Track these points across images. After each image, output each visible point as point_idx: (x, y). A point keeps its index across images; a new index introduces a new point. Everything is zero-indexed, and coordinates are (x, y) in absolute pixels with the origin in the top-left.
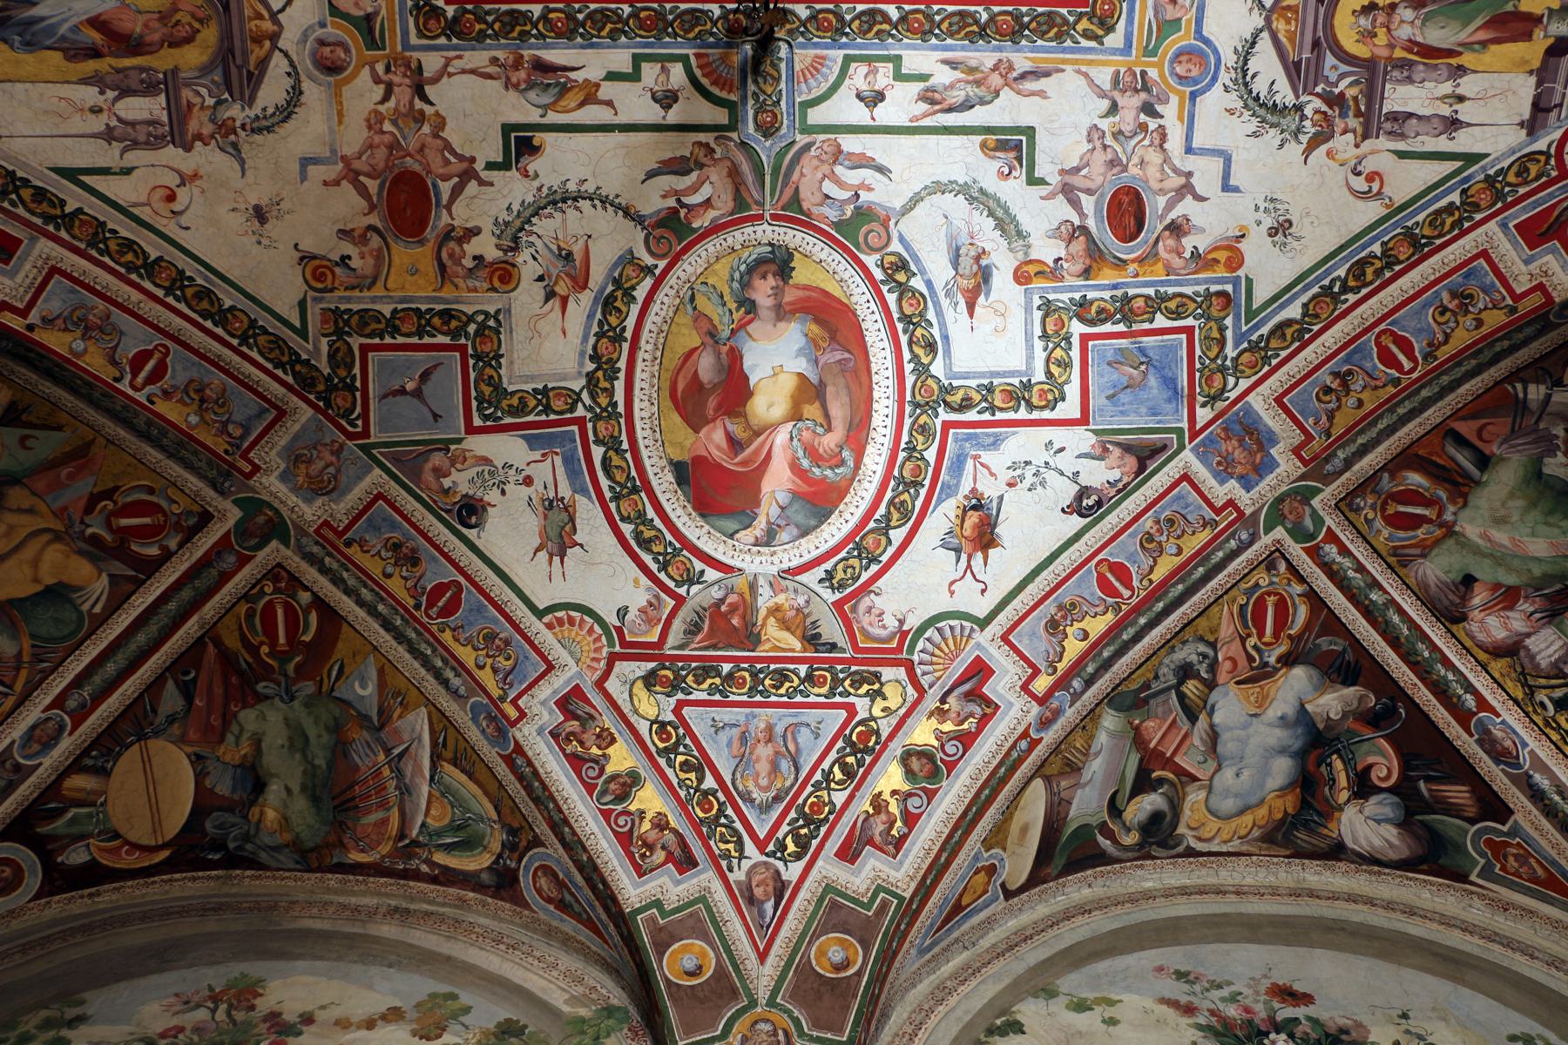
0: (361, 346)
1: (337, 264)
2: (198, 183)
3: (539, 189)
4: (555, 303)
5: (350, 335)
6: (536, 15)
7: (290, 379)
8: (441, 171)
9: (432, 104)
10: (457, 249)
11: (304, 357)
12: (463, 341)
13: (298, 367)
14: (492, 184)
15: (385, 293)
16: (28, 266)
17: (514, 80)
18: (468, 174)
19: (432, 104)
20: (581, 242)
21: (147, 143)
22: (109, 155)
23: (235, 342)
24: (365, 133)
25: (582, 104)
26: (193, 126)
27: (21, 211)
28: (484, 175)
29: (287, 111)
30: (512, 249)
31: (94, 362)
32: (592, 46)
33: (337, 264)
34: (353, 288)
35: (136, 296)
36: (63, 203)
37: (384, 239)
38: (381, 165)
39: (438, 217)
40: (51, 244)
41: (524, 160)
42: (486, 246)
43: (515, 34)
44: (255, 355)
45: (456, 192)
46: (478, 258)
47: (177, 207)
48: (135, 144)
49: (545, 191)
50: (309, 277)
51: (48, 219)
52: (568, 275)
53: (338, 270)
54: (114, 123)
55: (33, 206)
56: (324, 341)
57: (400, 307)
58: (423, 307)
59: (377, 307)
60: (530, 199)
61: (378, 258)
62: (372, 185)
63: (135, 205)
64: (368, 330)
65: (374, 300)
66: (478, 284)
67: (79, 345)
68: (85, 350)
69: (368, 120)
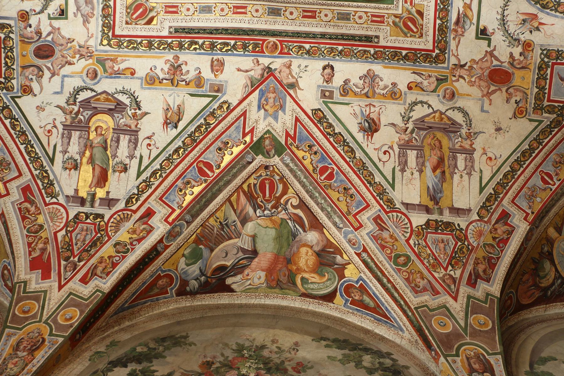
0: (548, 101)
1: (518, 105)
2: (486, 149)
3: (499, 29)
4: (541, 27)
5: (543, 105)
6: (440, 22)
7: (556, 130)
8: (489, 63)
9: (467, 63)
10: (517, 62)
11: (549, 123)
12: (550, 64)
13: (552, 126)
14: (495, 46)
15: (530, 90)
16: (511, 209)
17: (461, 33)
18: (491, 54)
19: (467, 63)
20: (519, 15)
21: (472, 163)
22: (476, 176)
23: (541, 147)
24: (475, 87)
25: (471, 10)
26: (468, 147)
27: (494, 207)
28: (492, 48)
29: (465, 114)
30: (519, 42)
31: (546, 195)
32: (452, 4)
33: (518, 105)
34: (527, 101)
35: (522, 177)
36: (491, 194)
37: (511, 87)
38: (486, 84)
39: (505, 67)
40: (504, 201)
41: (488, 33)
42: (517, 51)
43: (446, 30)
44: (546, 141)
45: (497, 59)
46: (521, 54)
47: (493, 157)
48: (472, 167)
49: (499, 27)
50: (521, 116)
51: (496, 200)
52: (531, 21)
53: (520, 105)
54: (465, 172)
55: (492, 203)
56: (544, 114)
57: (535, 85)
58: (536, 77)
59: (534, 93)
60: (502, 33)
61: (517, 90)
62: (492, 88)
63: (492, 171)
64: (542, 98)
65: (532, 94)
66: (530, 56)
67: (539, 200)
68: (540, 198)
69: (471, 86)
